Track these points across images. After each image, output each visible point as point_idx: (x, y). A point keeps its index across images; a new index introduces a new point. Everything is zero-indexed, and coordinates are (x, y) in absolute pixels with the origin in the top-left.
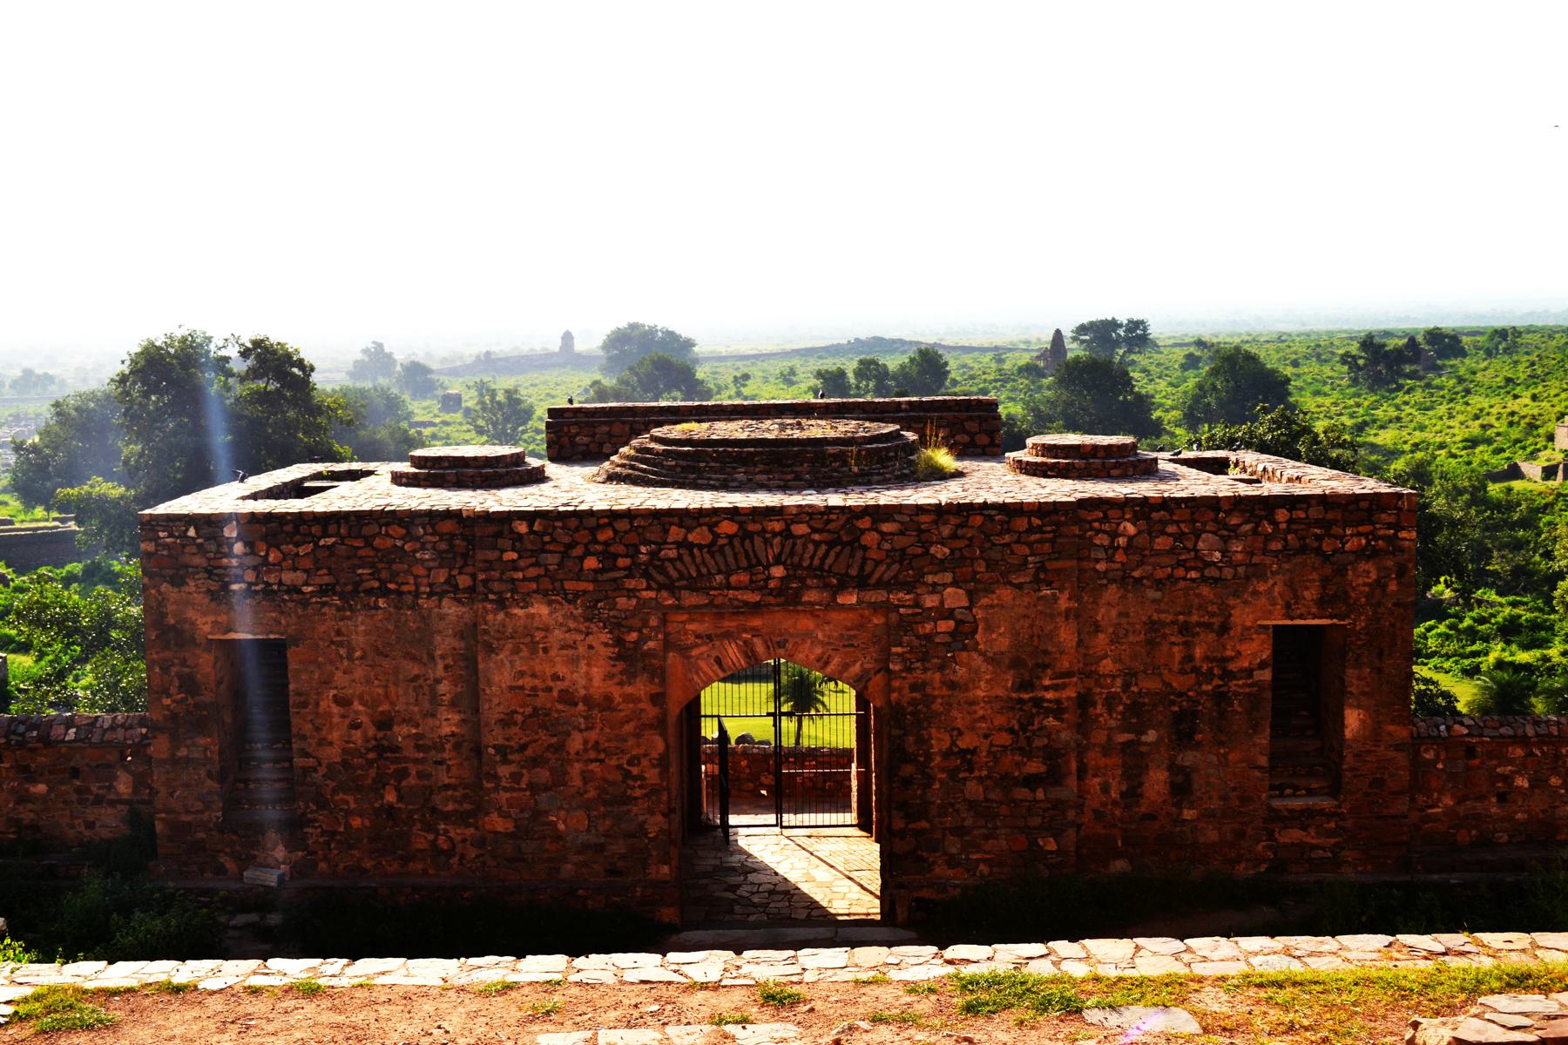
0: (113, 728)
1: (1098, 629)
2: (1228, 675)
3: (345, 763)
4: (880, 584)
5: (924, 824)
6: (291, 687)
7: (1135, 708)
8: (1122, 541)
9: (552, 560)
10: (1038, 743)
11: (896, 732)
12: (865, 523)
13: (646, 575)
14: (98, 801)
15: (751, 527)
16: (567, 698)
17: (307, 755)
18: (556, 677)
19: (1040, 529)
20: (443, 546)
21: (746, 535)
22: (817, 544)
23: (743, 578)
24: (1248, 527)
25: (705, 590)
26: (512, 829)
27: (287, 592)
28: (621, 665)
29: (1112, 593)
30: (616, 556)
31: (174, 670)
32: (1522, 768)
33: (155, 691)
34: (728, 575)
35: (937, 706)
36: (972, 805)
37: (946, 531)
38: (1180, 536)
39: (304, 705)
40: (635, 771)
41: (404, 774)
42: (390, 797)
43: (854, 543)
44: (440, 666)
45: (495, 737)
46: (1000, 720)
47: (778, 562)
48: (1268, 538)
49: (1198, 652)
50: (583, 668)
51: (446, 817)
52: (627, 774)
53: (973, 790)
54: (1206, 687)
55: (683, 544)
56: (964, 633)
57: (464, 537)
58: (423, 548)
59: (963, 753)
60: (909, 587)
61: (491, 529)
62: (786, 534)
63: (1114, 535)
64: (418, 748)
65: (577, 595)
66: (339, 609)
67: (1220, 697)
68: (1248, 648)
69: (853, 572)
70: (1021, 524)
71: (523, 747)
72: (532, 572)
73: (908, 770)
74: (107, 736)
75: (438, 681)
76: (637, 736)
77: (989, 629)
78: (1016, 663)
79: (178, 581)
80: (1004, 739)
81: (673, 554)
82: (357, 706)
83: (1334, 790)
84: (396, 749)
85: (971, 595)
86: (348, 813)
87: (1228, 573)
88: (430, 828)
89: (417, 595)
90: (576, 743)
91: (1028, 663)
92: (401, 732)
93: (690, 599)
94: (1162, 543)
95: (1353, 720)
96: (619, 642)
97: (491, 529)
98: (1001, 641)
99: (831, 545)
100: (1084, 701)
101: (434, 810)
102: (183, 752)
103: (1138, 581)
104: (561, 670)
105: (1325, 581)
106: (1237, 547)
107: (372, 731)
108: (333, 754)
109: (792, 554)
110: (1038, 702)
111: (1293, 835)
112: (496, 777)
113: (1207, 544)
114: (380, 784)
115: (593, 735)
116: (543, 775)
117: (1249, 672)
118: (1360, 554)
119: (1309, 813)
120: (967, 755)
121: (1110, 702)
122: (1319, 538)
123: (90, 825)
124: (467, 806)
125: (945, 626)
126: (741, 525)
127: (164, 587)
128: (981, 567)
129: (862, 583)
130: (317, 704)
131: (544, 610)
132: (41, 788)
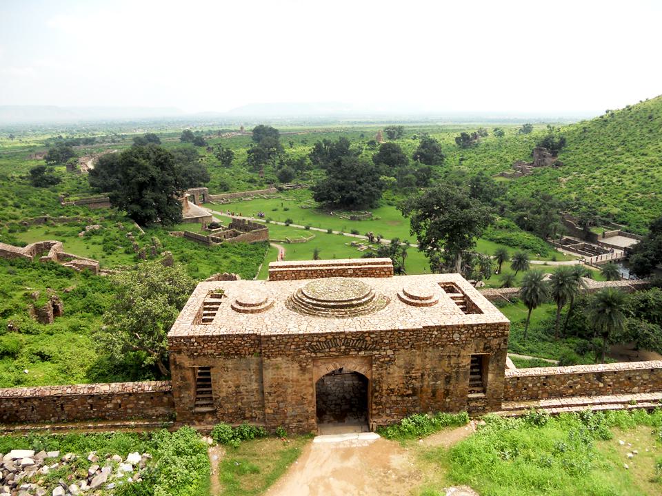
0: (162, 386)
1: (426, 357)
2: (460, 367)
3: (227, 397)
4: (370, 349)
5: (381, 407)
7: (435, 376)
8: (434, 336)
10: (410, 386)
11: (374, 385)
12: (367, 334)
13: (308, 349)
15: (336, 337)
16: (287, 380)
18: (284, 375)
19: (412, 335)
20: (252, 342)
22: (354, 340)
24: (466, 332)
25: (324, 353)
26: (272, 411)
28: (301, 372)
30: (299, 345)
31: (179, 376)
32: (531, 382)
34: (330, 348)
35: (384, 379)
36: (393, 402)
37: (388, 336)
38: (449, 334)
39: (216, 383)
40: (305, 397)
41: (242, 399)
42: (239, 404)
43: (364, 340)
44: (252, 371)
45: (266, 390)
46: (401, 381)
47: (343, 345)
48: (471, 334)
49: (452, 362)
50: (291, 372)
51: (255, 408)
52: (303, 398)
53: (394, 398)
54: (454, 370)
55: (318, 341)
57: (258, 340)
58: (247, 343)
59: (391, 390)
60: (378, 350)
61: (266, 339)
62: (346, 338)
63: (431, 335)
64: (247, 392)
65: (289, 355)
66: (224, 359)
67: (457, 373)
68: (464, 361)
69: (363, 347)
70: (408, 334)
71: (275, 393)
72: (277, 349)
73: (376, 394)
74: (161, 388)
75: (252, 375)
76: (305, 388)
77: (399, 360)
78: (405, 368)
80: (402, 386)
81: (315, 344)
82: (230, 382)
83: (484, 391)
84: (240, 392)
85: (394, 351)
86: (228, 409)
87: (461, 343)
88: (251, 411)
89: (245, 355)
90: (289, 391)
91: (409, 367)
92: (242, 389)
93: (319, 355)
94: (444, 336)
95: (490, 376)
96: (301, 366)
97: (266, 339)
99: (357, 340)
100: (422, 375)
101: (251, 407)
103: (437, 346)
104: (285, 373)
105: (485, 344)
106: (463, 336)
107: (234, 388)
108: (224, 394)
109: (347, 343)
110: (410, 377)
111: (474, 404)
112: (268, 400)
113: (456, 337)
114: (237, 401)
115: (294, 389)
116: (280, 399)
117: (465, 366)
118: (494, 337)
119: (478, 399)
120: (392, 391)
121: (429, 376)
122: (484, 333)
124: (260, 406)
125: (387, 359)
126: (333, 336)
127: (176, 354)
128: (397, 344)
129: (366, 349)
131: (280, 359)
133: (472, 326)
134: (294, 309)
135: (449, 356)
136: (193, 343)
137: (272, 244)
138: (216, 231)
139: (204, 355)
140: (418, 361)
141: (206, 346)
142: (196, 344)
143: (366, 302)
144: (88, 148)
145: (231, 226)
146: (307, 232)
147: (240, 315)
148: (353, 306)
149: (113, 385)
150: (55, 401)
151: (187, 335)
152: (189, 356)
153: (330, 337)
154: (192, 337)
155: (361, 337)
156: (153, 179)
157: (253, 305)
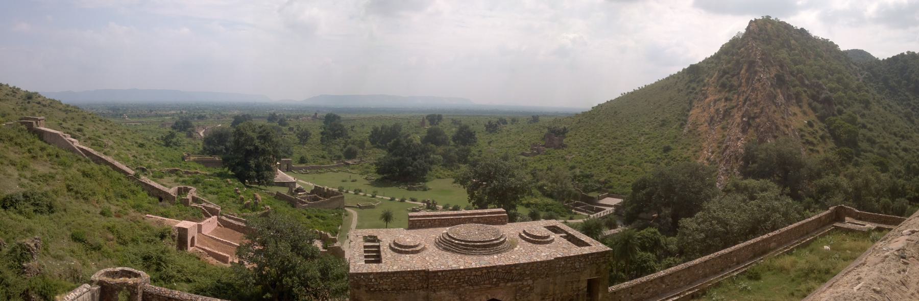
9: (446, 281)
21: (488, 272)
23: (487, 282)
29: (559, 277)
43: (511, 272)
56: (532, 289)
62: (497, 272)
67: (578, 295)
78: (541, 294)
79: (358, 288)
93: (476, 287)
94: (569, 265)
98: (538, 290)
113: (577, 265)
129: (512, 280)
133: (588, 255)
134: (446, 249)
135: (572, 282)
139: (380, 290)
140: (551, 287)
143: (503, 242)
144: (201, 123)
147: (403, 255)
148: (494, 245)
153: (485, 271)
155: (508, 269)
156: (257, 148)
157: (412, 247)
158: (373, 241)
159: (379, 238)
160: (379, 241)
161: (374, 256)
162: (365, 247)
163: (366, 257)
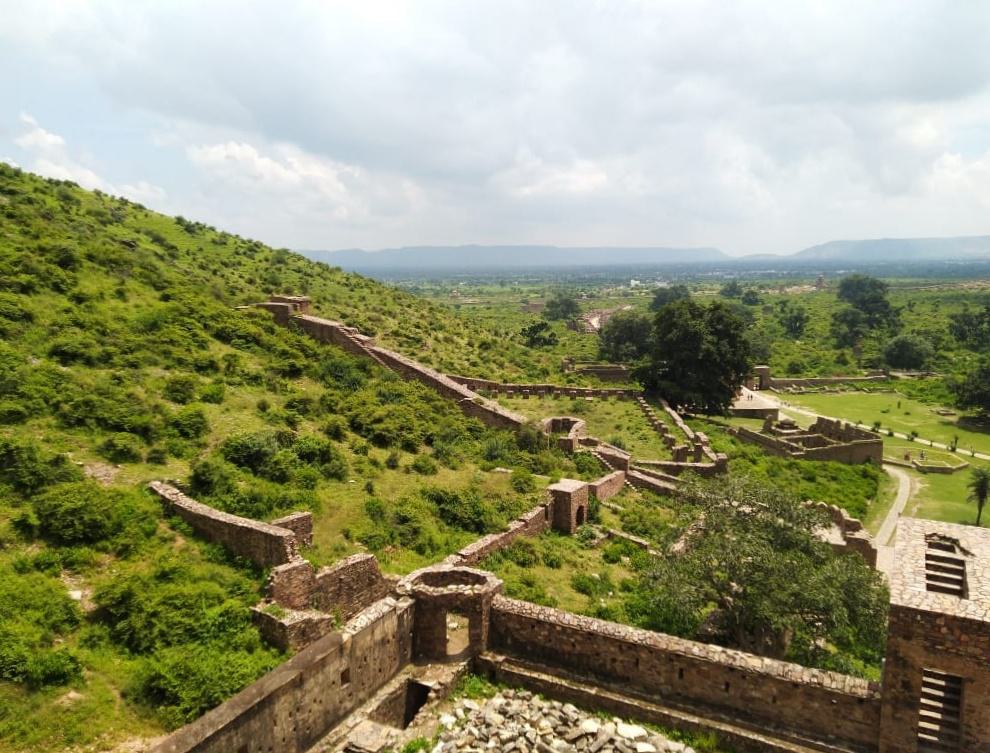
6: (966, 701)
14: (844, 718)
17: (968, 733)
27: (970, 657)
31: (900, 677)
33: (887, 685)
39: (973, 712)
74: (854, 690)
79: (908, 637)
102: (898, 715)
123: (838, 727)
127: (900, 639)
130: (980, 713)
132: (816, 705)
136: (940, 627)
137: (885, 467)
138: (788, 434)
141: (964, 638)
142: (944, 630)
145: (813, 429)
146: (953, 455)
149: (767, 661)
150: (671, 660)
151: (928, 609)
152: (926, 648)
154: (940, 615)
158: (951, 549)
159: (963, 544)
160: (965, 552)
161: (946, 573)
162: (928, 557)
163: (929, 577)
